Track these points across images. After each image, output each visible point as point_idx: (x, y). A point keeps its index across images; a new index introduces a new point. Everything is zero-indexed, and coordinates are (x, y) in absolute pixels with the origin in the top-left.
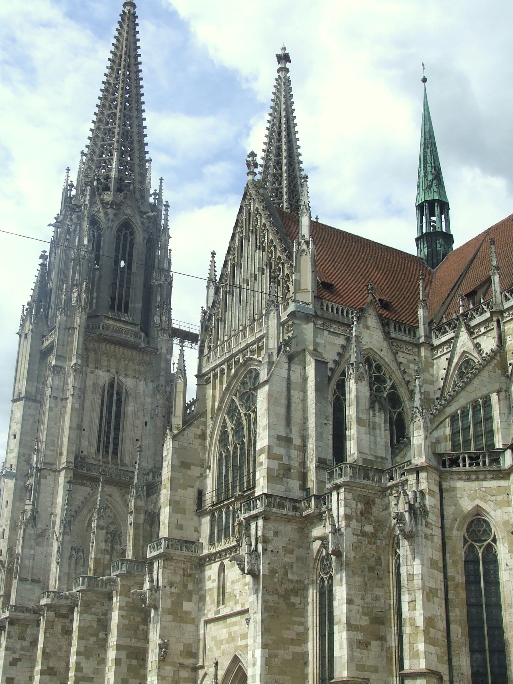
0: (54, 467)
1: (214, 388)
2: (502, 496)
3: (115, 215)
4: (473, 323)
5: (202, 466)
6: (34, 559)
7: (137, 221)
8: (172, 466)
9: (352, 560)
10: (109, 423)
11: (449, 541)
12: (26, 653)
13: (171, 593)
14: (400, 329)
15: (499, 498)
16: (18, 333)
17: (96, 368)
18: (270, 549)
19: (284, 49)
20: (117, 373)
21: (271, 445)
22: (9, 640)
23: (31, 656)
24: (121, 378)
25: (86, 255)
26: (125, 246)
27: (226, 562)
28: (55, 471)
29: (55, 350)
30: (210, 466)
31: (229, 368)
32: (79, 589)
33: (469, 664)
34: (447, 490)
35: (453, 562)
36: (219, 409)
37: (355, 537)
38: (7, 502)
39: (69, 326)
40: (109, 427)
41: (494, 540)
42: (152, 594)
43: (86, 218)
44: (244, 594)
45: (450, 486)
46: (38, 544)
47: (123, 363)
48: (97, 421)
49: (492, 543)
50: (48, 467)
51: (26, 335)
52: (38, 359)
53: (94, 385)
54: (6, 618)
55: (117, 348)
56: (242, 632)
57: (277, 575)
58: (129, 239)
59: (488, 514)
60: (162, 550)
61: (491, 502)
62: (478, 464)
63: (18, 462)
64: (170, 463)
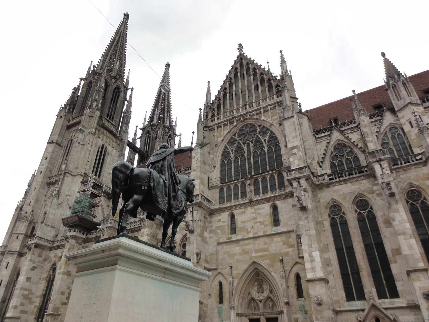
0: (73, 174)
1: (217, 133)
3: (115, 82)
4: (342, 129)
5: (209, 166)
6: (54, 216)
7: (122, 88)
8: (200, 161)
10: (99, 163)
12: (41, 265)
13: (201, 225)
16: (56, 115)
17: (98, 137)
19: (168, 63)
20: (106, 142)
22: (33, 256)
23: (43, 266)
24: (107, 146)
26: (116, 96)
27: (235, 212)
28: (72, 175)
29: (82, 123)
30: (215, 167)
31: (231, 123)
32: (107, 226)
36: (222, 141)
38: (35, 188)
39: (90, 116)
40: (98, 165)
42: (192, 223)
43: (103, 77)
44: (256, 227)
46: (58, 208)
47: (108, 140)
48: (95, 160)
50: (70, 172)
51: (61, 117)
52: (65, 129)
53: (96, 144)
54: (33, 244)
55: (108, 133)
56: (256, 248)
58: (118, 94)
60: (200, 200)
63: (46, 170)
64: (199, 159)
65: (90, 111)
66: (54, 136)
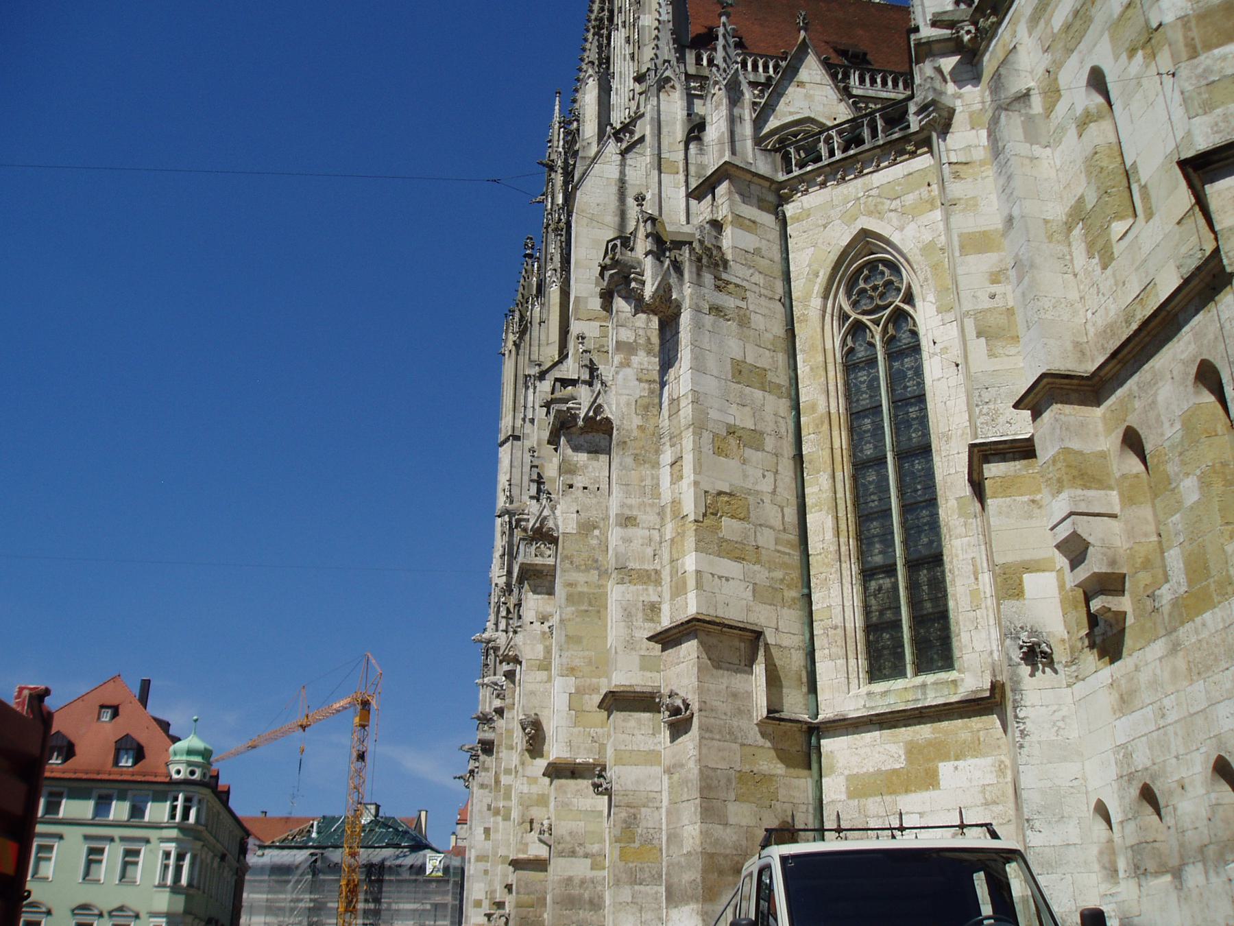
2: (918, 192)
9: (635, 433)
11: (803, 325)
14: (873, 82)
15: (910, 199)
18: (581, 485)
21: (584, 294)
25: (562, 217)
33: (858, 602)
34: (798, 219)
35: (812, 369)
37: (646, 386)
41: (909, 298)
45: (802, 208)
49: (902, 305)
57: (596, 532)
59: (888, 242)
61: (892, 214)
62: (859, 142)
65: (542, 305)
66: (507, 418)
